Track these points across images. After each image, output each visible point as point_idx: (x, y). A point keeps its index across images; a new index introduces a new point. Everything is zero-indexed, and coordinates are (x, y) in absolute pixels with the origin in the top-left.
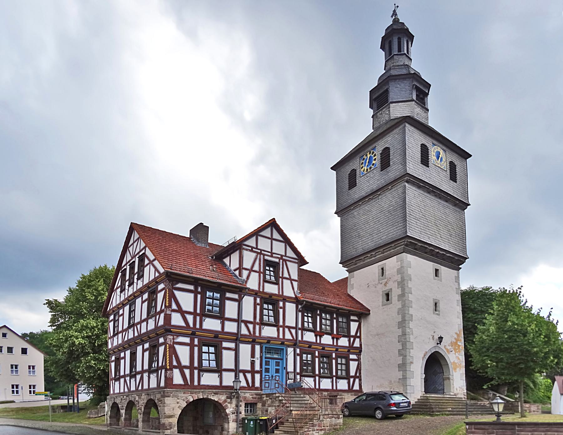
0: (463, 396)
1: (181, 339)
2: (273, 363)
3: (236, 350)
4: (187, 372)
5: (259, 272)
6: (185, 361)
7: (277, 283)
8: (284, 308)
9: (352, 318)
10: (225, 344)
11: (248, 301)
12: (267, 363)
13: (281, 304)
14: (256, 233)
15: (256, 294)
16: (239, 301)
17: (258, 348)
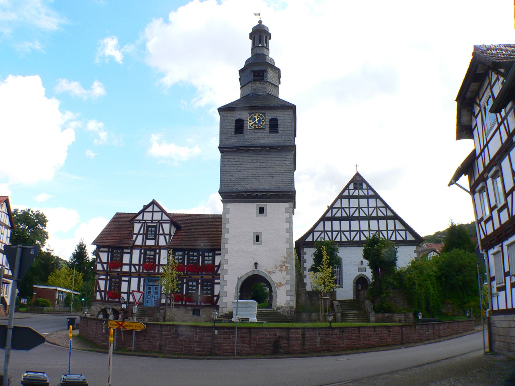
0: (298, 348)
1: (102, 277)
2: (153, 288)
3: (129, 282)
4: (103, 293)
5: (143, 234)
6: (102, 288)
7: (154, 239)
8: (159, 254)
9: (123, 278)
10: (123, 278)
11: (136, 253)
12: (150, 288)
13: (158, 251)
14: (143, 211)
15: (141, 247)
16: (131, 254)
17: (142, 280)
